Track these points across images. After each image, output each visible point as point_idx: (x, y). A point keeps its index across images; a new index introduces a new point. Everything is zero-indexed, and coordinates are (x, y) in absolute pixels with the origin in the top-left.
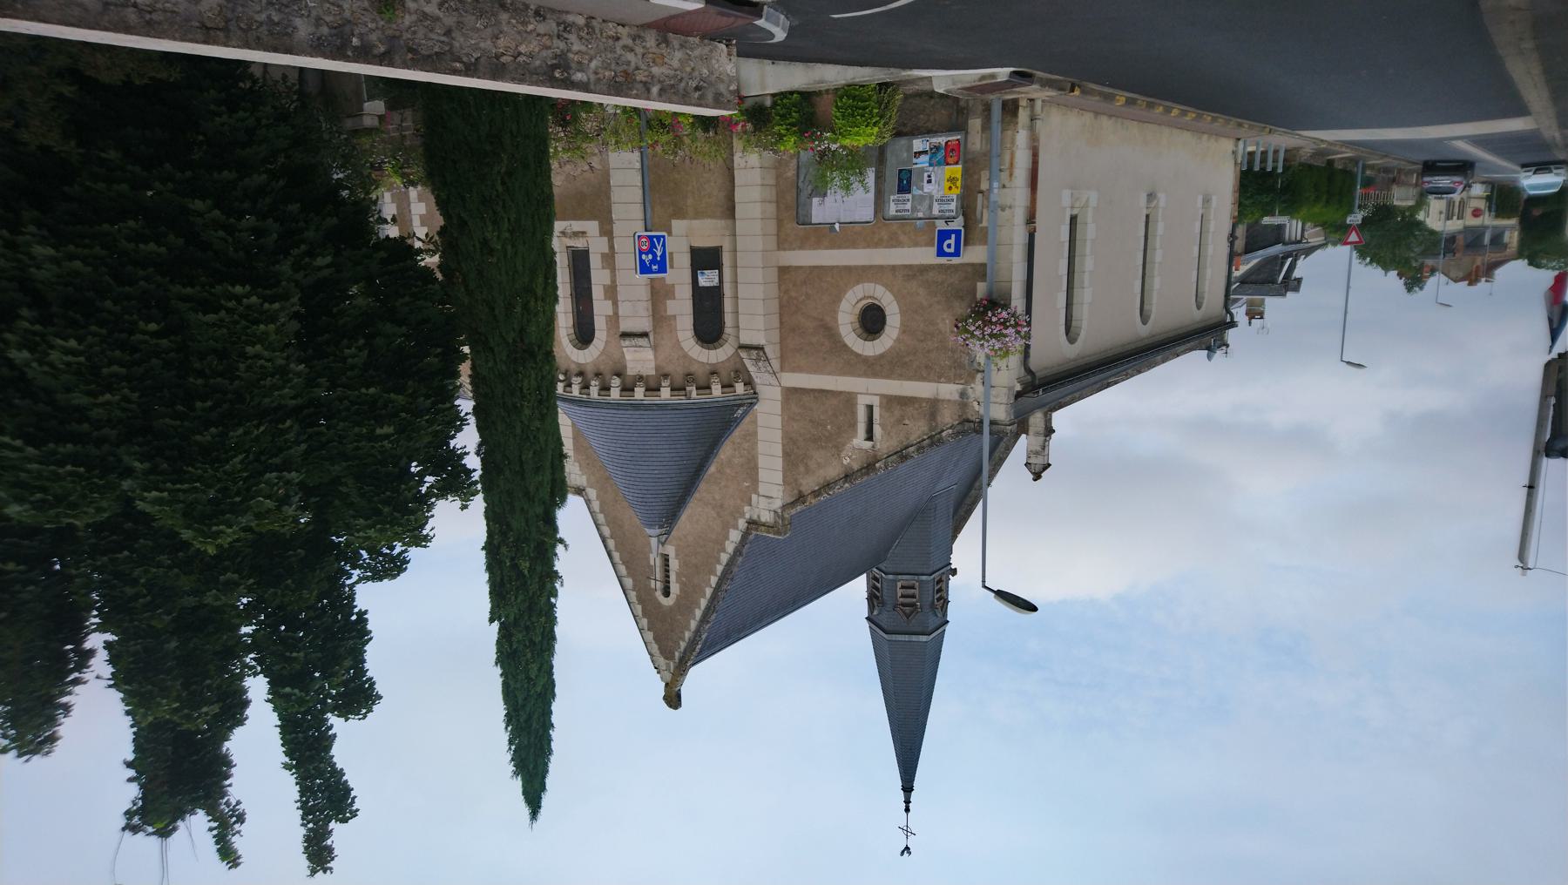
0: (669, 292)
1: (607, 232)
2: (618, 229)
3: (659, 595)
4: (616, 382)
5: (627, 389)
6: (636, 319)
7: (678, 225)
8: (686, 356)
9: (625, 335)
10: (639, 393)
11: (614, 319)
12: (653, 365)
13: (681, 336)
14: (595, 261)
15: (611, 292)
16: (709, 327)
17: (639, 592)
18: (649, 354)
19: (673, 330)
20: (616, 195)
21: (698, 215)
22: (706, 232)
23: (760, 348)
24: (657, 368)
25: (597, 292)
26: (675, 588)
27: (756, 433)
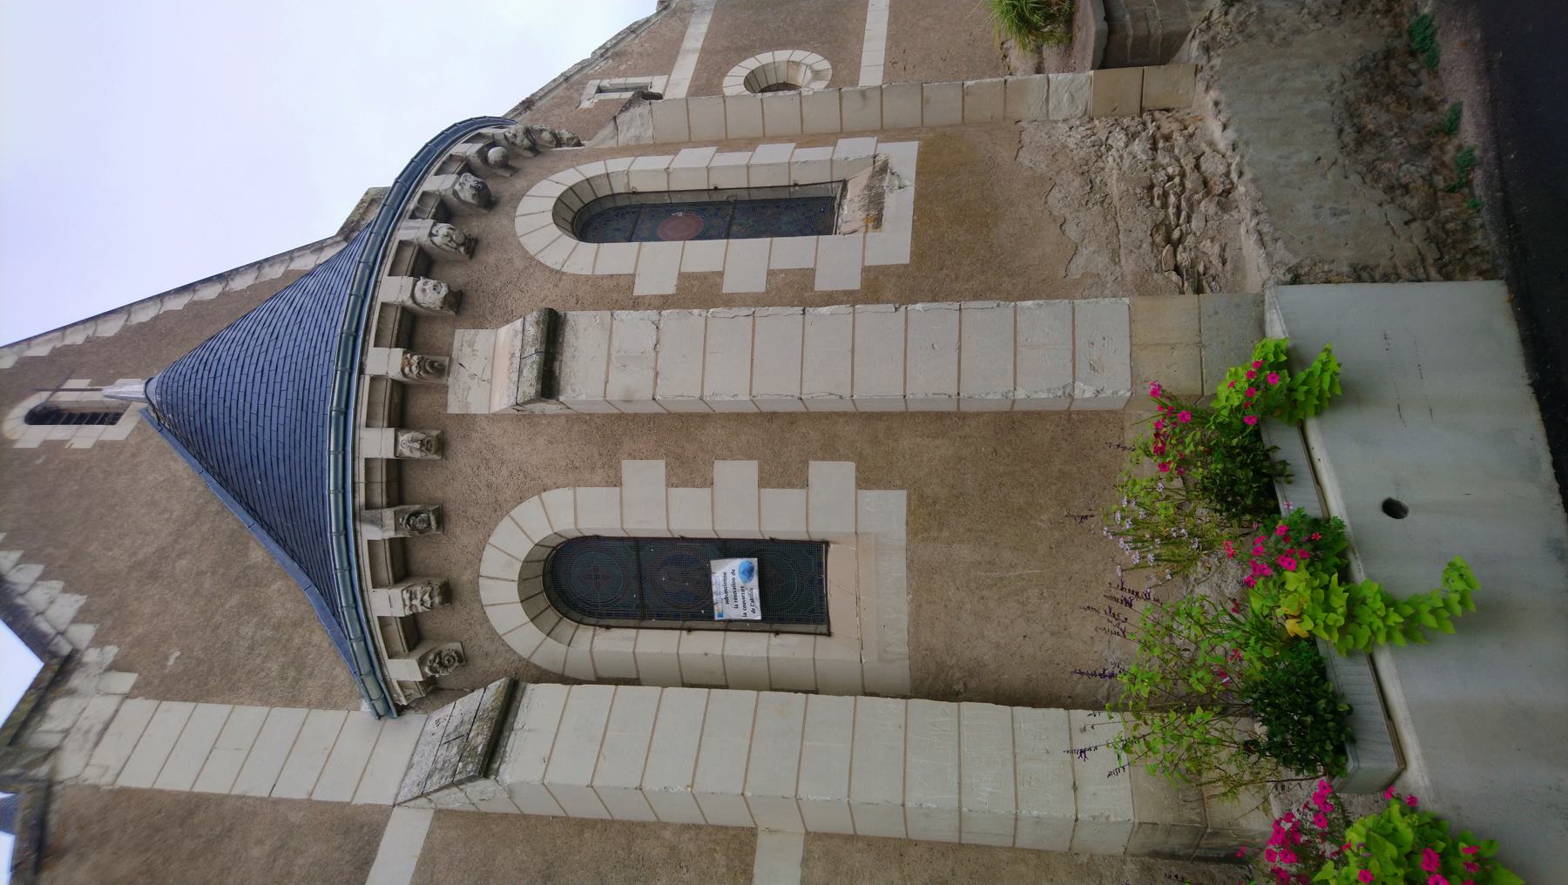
0: (688, 472)
1: (878, 286)
2: (879, 318)
3: (34, 401)
4: (430, 294)
5: (410, 329)
6: (603, 364)
7: (888, 510)
8: (499, 510)
9: (553, 328)
10: (385, 362)
11: (616, 295)
12: (477, 406)
13: (560, 499)
14: (792, 251)
15: (699, 292)
16: (577, 580)
17: (76, 350)
18: (502, 400)
19: (574, 475)
20: (986, 317)
21: (921, 574)
22: (871, 595)
23: (489, 761)
24: (466, 420)
25: (704, 255)
26: (37, 435)
27: (292, 701)
